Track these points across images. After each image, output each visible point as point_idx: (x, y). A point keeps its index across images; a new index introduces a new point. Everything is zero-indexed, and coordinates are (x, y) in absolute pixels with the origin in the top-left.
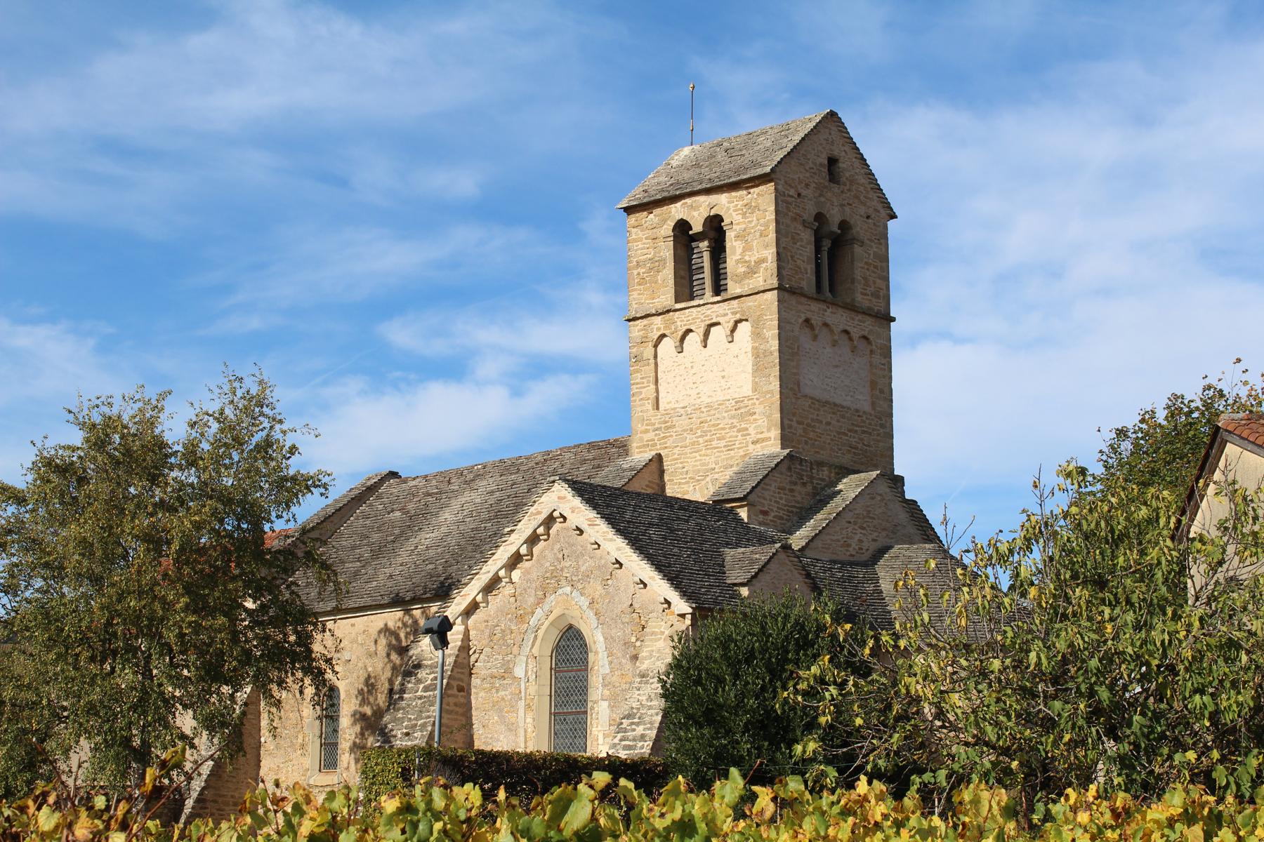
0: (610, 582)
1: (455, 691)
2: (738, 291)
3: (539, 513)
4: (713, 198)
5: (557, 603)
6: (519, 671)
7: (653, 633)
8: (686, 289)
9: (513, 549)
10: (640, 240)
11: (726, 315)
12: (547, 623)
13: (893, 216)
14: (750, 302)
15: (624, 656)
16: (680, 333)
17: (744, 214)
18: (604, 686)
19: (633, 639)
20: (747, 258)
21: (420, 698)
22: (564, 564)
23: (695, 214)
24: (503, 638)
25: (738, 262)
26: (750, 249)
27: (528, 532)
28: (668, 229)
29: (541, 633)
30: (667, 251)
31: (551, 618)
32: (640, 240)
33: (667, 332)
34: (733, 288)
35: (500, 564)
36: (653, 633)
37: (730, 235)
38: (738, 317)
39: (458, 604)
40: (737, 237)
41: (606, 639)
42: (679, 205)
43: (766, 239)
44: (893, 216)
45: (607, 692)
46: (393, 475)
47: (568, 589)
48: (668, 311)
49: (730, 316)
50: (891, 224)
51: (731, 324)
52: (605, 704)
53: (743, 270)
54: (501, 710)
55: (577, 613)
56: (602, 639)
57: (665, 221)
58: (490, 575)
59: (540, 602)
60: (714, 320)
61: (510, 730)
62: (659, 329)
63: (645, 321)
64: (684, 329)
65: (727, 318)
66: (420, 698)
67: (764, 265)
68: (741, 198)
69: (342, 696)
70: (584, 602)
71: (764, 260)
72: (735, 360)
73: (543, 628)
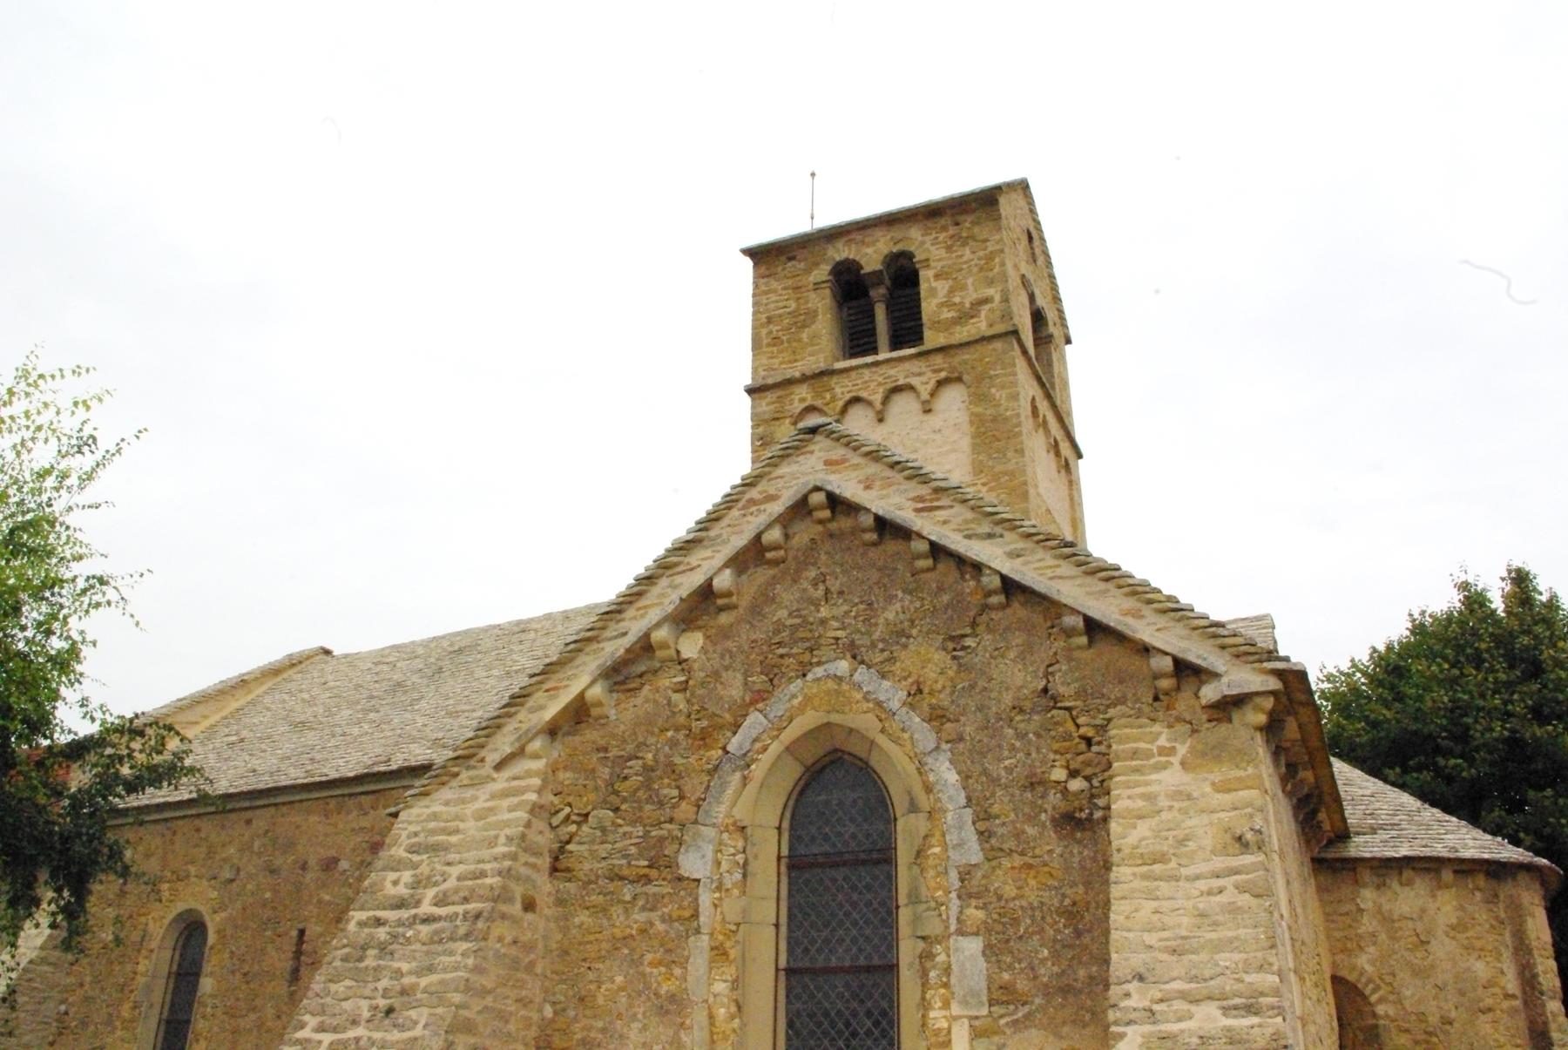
0: (969, 642)
1: (516, 908)
2: (941, 340)
3: (771, 498)
4: (897, 232)
5: (808, 700)
6: (693, 863)
7: (1135, 754)
8: (858, 340)
9: (697, 579)
10: (775, 291)
11: (920, 374)
12: (775, 748)
13: (1068, 341)
14: (966, 356)
15: (1031, 819)
16: (841, 403)
17: (949, 249)
18: (965, 896)
19: (1059, 774)
20: (957, 300)
21: (427, 920)
22: (824, 612)
23: (869, 250)
24: (647, 785)
25: (942, 305)
26: (964, 288)
27: (740, 541)
28: (822, 272)
29: (758, 770)
30: (822, 304)
31: (789, 735)
32: (775, 291)
33: (818, 403)
34: (932, 338)
35: (654, 615)
36: (1135, 754)
37: (926, 276)
38: (943, 375)
39: (532, 711)
40: (937, 277)
41: (966, 777)
42: (840, 244)
43: (990, 274)
44: (1068, 341)
45: (975, 914)
46: (327, 652)
47: (843, 666)
48: (822, 373)
49: (929, 374)
50: (1068, 347)
51: (933, 383)
52: (972, 946)
53: (950, 315)
54: (636, 962)
55: (866, 722)
56: (953, 777)
57: (817, 264)
58: (627, 642)
59: (759, 698)
60: (901, 382)
61: (662, 1012)
62: (803, 400)
63: (780, 393)
64: (848, 397)
65: (924, 379)
66: (427, 920)
67: (987, 307)
68: (944, 228)
69: (212, 938)
70: (893, 694)
71: (986, 301)
72: (937, 437)
73: (766, 759)
